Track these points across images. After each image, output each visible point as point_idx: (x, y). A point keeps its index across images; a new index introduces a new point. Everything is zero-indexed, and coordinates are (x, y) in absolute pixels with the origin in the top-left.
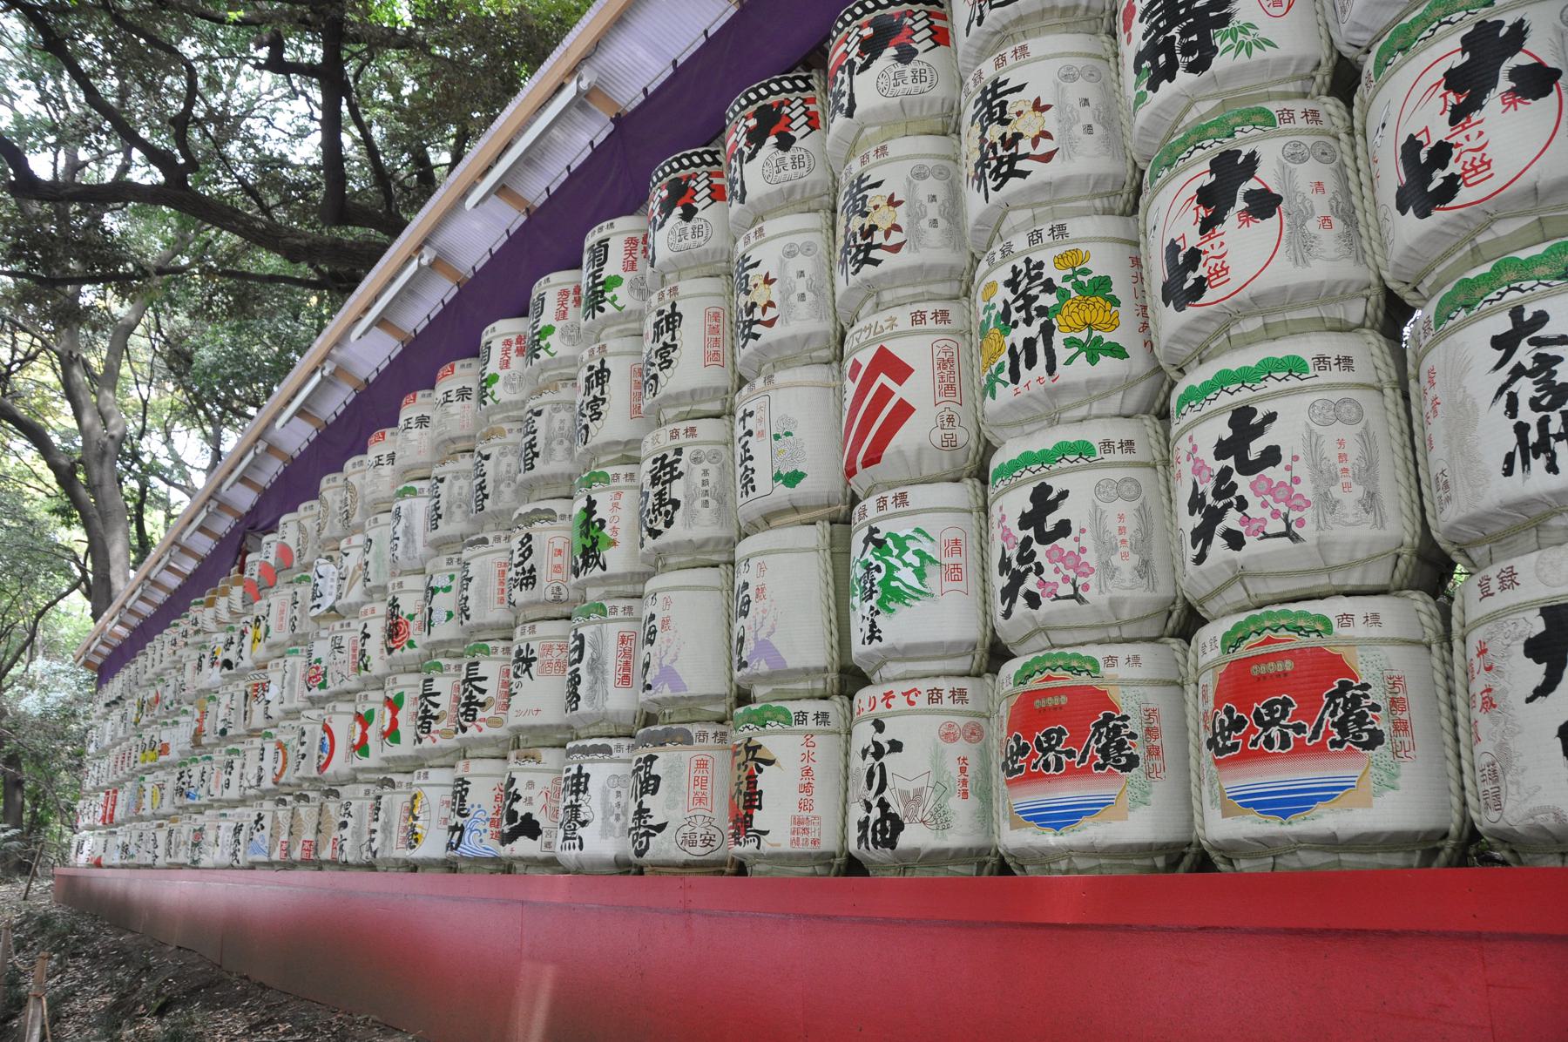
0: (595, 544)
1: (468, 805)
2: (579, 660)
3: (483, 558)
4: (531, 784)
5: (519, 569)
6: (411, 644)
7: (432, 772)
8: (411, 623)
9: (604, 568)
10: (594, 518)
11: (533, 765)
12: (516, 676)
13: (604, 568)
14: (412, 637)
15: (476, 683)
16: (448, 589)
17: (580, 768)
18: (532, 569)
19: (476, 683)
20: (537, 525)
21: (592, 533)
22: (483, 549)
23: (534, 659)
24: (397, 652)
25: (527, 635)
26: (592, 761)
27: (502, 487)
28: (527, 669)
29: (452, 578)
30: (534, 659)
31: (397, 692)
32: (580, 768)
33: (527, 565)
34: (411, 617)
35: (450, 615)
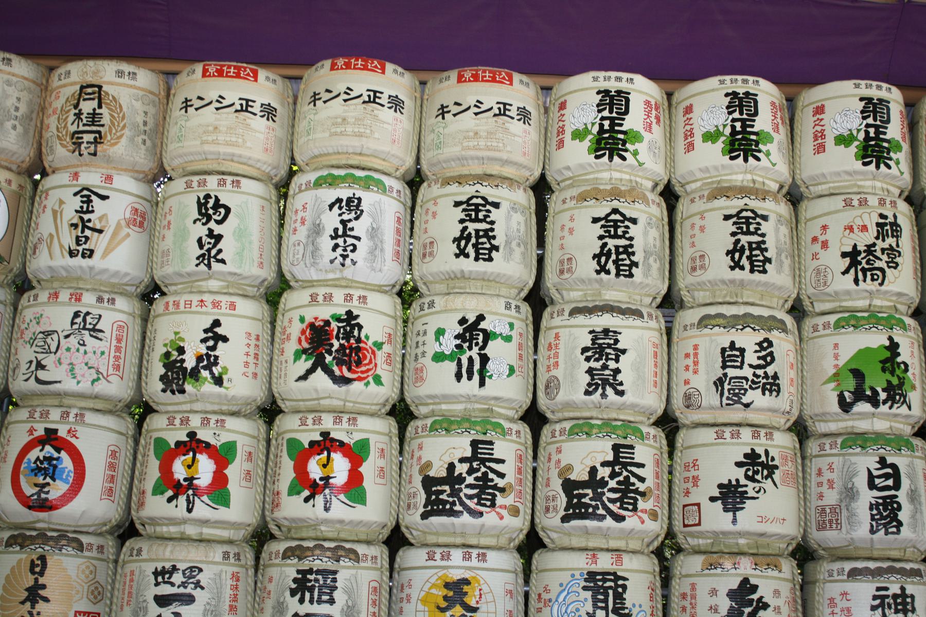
0: (901, 384)
1: (628, 604)
2: (897, 486)
3: (640, 332)
4: (777, 593)
5: (760, 372)
6: (378, 380)
7: (491, 555)
8: (379, 353)
9: (909, 408)
10: (899, 359)
11: (775, 573)
12: (752, 479)
13: (909, 408)
14: (379, 371)
15: (634, 469)
16: (508, 339)
17: (903, 589)
18: (776, 377)
19: (634, 469)
20: (775, 332)
21: (898, 372)
22: (638, 322)
23: (776, 467)
24: (357, 386)
25: (763, 440)
26: (913, 583)
27: (651, 260)
28: (770, 475)
29: (511, 326)
30: (776, 467)
31: (357, 436)
32: (903, 589)
33: (770, 370)
34: (379, 345)
35: (512, 370)
